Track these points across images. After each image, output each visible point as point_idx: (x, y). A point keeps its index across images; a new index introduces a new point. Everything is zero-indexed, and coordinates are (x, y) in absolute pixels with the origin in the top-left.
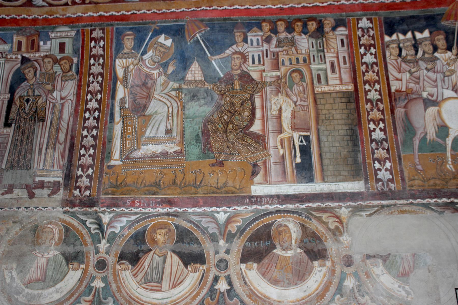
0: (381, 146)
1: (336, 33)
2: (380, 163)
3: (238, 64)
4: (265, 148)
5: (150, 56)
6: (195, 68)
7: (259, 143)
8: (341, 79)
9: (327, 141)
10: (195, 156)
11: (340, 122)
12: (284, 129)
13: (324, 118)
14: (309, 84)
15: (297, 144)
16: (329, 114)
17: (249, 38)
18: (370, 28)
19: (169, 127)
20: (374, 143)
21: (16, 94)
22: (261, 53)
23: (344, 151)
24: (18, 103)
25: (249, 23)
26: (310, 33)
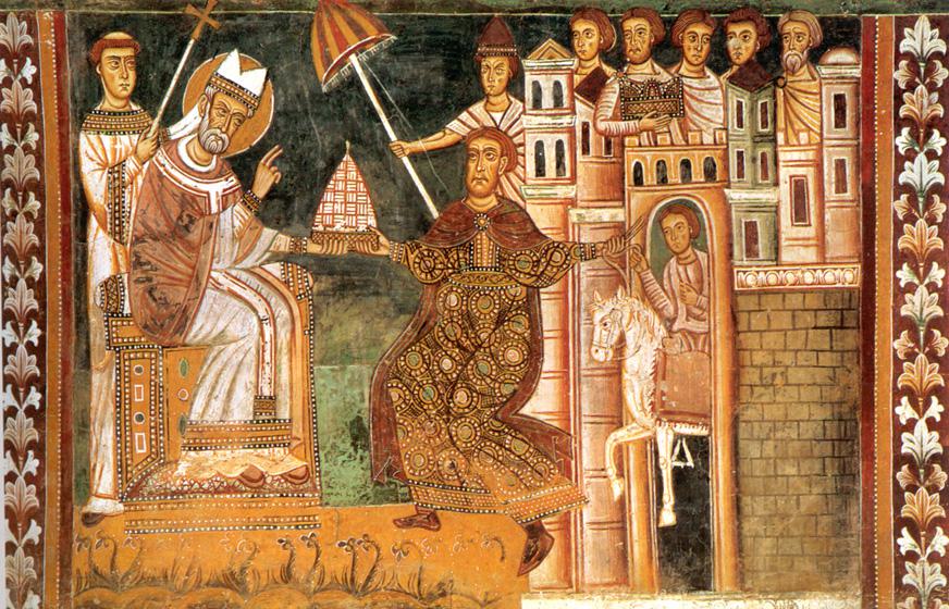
0: (927, 476)
1: (824, 71)
2: (915, 534)
3: (489, 174)
4: (566, 471)
5: (190, 128)
6: (346, 180)
7: (547, 456)
8: (821, 244)
9: (761, 458)
10: (351, 492)
11: (806, 394)
12: (628, 411)
13: (755, 379)
14: (716, 255)
15: (668, 463)
16: (774, 366)
17: (529, 78)
18: (938, 55)
19: (267, 392)
20: (905, 468)
22: (564, 137)
23: (810, 493)
25: (532, 20)
26: (735, 68)
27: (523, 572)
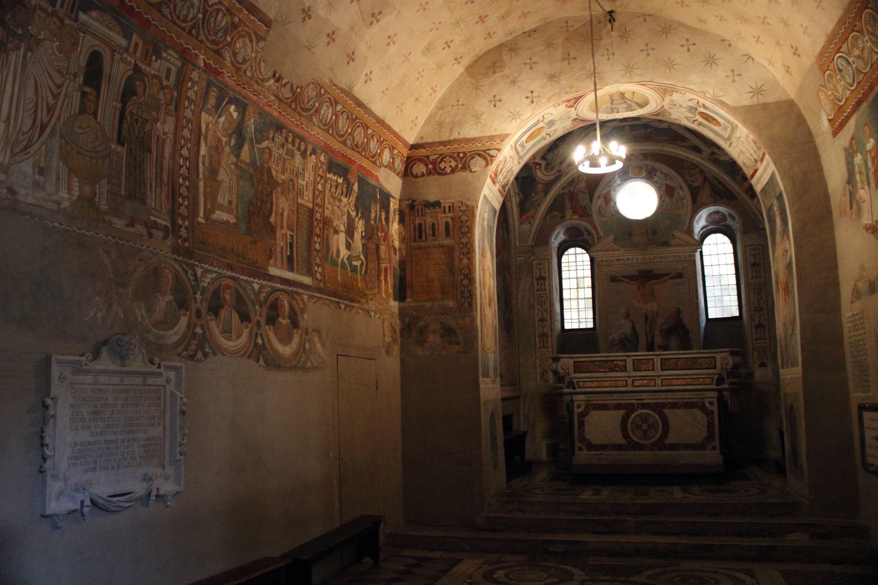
21: (127, 106)
24: (129, 119)
27: (269, 261)
